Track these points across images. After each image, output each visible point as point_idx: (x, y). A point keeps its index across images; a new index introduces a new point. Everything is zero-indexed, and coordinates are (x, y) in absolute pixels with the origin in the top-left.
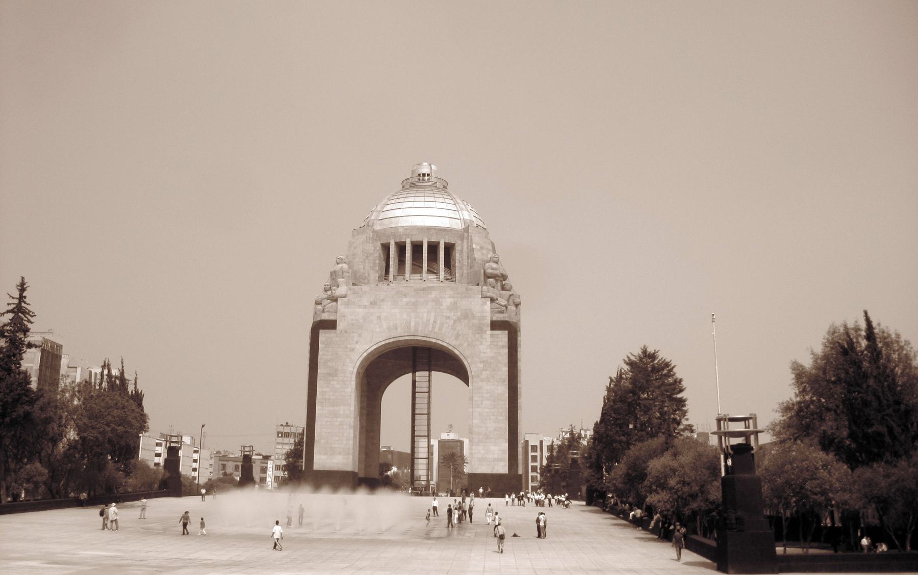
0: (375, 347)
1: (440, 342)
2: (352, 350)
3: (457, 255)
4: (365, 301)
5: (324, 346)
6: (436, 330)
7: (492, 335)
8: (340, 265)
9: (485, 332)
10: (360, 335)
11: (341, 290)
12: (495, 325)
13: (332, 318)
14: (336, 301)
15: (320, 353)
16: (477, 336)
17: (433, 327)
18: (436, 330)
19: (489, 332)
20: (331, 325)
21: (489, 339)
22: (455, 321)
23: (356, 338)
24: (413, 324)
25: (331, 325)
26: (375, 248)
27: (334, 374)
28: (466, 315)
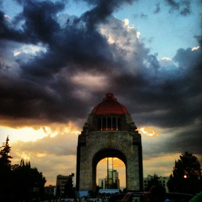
1: (117, 149)
2: (91, 152)
3: (122, 122)
4: (94, 136)
6: (117, 145)
7: (133, 147)
8: (86, 126)
9: (131, 146)
10: (93, 147)
11: (87, 133)
12: (134, 144)
14: (85, 137)
17: (116, 144)
19: (132, 146)
21: (132, 148)
27: (85, 160)
28: (126, 140)
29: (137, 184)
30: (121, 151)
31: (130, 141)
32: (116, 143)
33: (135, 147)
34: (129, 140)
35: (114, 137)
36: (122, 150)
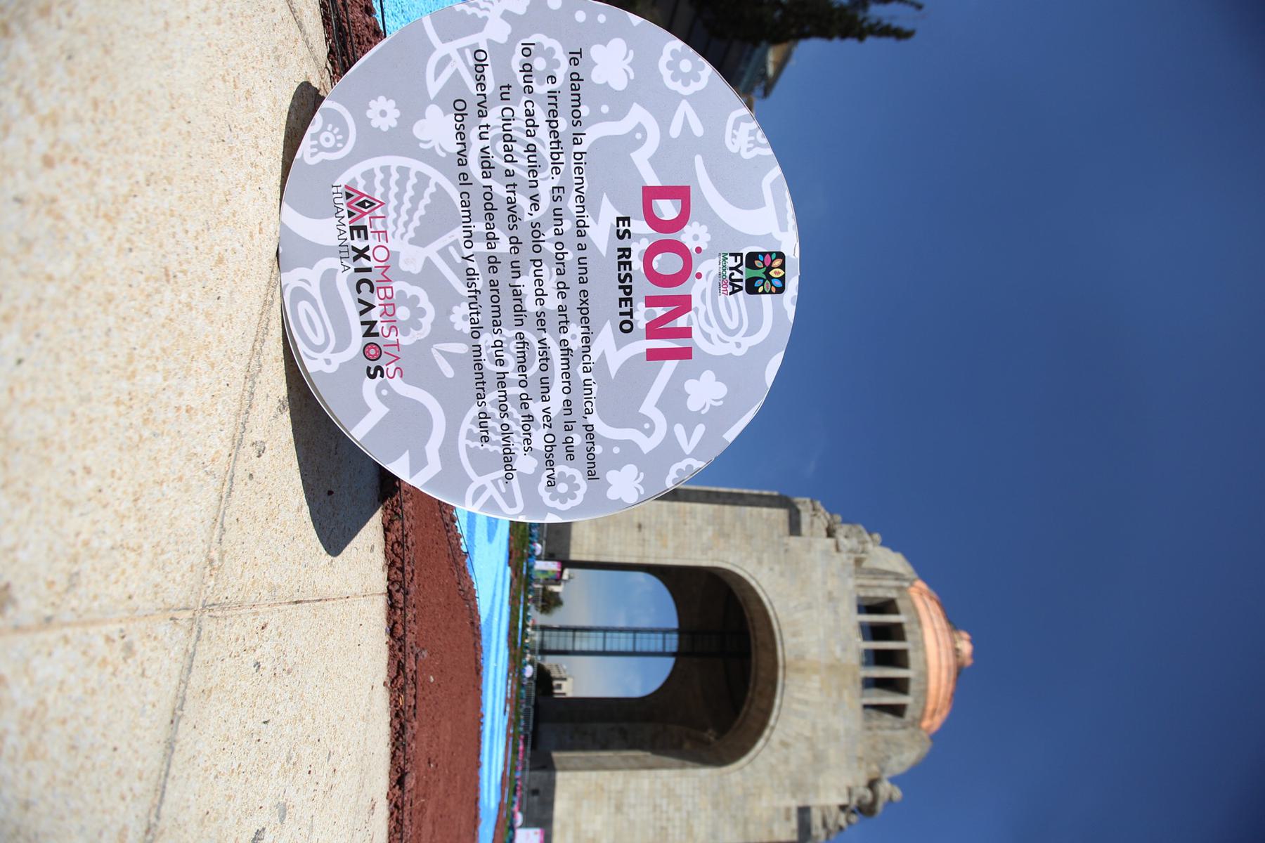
0: (765, 600)
4: (832, 584)
5: (765, 516)
6: (795, 706)
7: (788, 810)
9: (794, 795)
10: (782, 574)
12: (804, 812)
13: (805, 528)
15: (755, 510)
16: (787, 782)
17: (800, 701)
18: (795, 706)
19: (794, 804)
20: (794, 528)
22: (808, 739)
23: (777, 568)
24: (802, 664)
25: (794, 528)
26: (890, 588)
27: (722, 534)
29: (590, 835)
30: (767, 732)
31: (816, 789)
32: (806, 703)
33: (788, 819)
34: (821, 782)
35: (834, 694)
36: (768, 740)
